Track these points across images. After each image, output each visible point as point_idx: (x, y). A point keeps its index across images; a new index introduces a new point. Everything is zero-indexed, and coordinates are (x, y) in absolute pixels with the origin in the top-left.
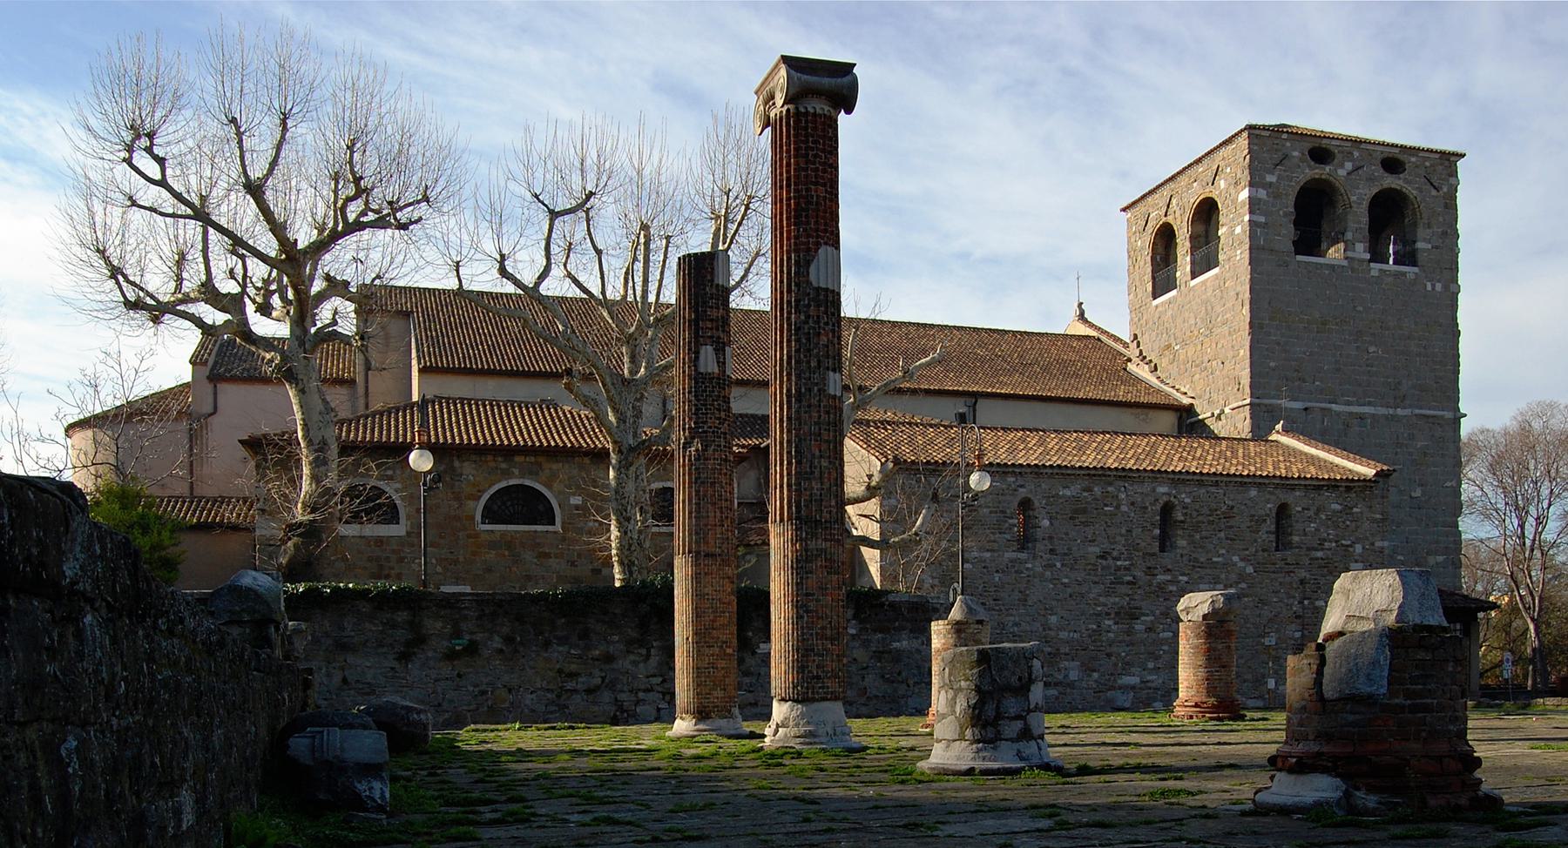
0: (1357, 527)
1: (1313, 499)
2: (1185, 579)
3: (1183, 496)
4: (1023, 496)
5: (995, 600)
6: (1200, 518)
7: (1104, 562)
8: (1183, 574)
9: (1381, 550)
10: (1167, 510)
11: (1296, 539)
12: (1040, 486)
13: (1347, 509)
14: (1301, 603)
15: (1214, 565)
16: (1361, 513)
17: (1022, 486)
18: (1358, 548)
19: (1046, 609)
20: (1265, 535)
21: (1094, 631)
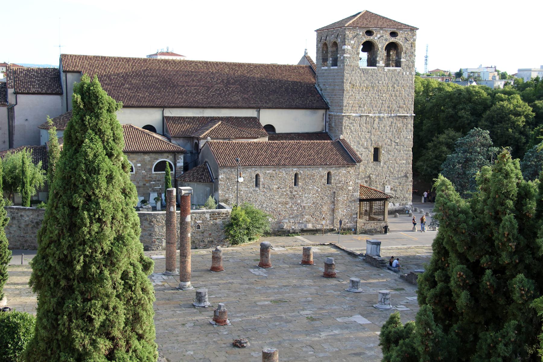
8: (300, 192)
14: (334, 198)
18: (351, 183)
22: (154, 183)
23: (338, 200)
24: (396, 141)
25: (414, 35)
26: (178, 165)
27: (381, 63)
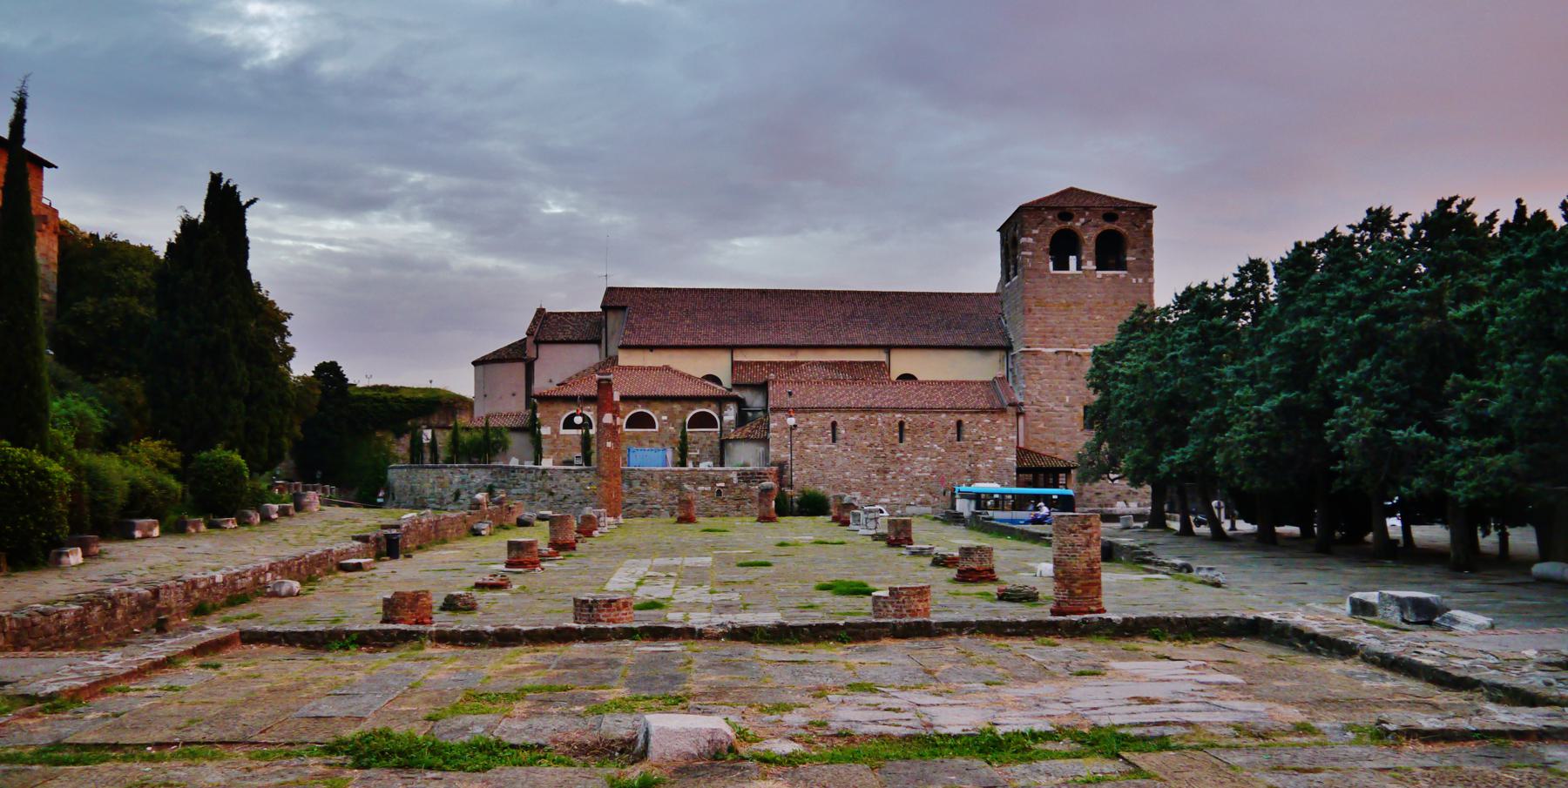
2: (909, 455)
10: (901, 424)
11: (966, 436)
13: (993, 422)
15: (925, 449)
18: (1000, 440)
20: (952, 432)
23: (978, 469)
25: (1150, 217)
26: (725, 418)
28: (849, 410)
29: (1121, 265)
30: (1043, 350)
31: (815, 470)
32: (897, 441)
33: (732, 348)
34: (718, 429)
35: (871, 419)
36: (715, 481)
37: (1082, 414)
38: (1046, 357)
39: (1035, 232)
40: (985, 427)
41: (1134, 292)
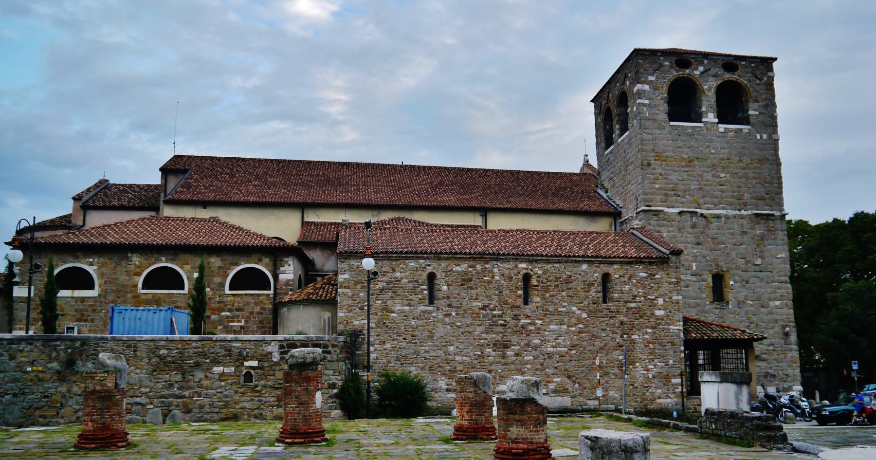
0: (659, 287)
1: (626, 270)
2: (540, 322)
3: (537, 269)
4: (430, 271)
5: (412, 336)
6: (549, 283)
7: (483, 312)
8: (539, 319)
9: (677, 302)
10: (527, 278)
12: (440, 265)
14: (622, 337)
16: (661, 278)
17: (429, 265)
18: (660, 301)
19: (447, 342)
20: (595, 292)
21: (479, 356)
22: (228, 314)
24: (756, 263)
25: (771, 69)
26: (282, 277)
27: (711, 117)
28: (454, 256)
29: (746, 121)
30: (666, 210)
31: (404, 344)
32: (520, 302)
33: (302, 207)
34: (271, 292)
35: (484, 270)
36: (242, 358)
37: (711, 284)
38: (668, 218)
39: (651, 78)
40: (641, 282)
41: (761, 149)
